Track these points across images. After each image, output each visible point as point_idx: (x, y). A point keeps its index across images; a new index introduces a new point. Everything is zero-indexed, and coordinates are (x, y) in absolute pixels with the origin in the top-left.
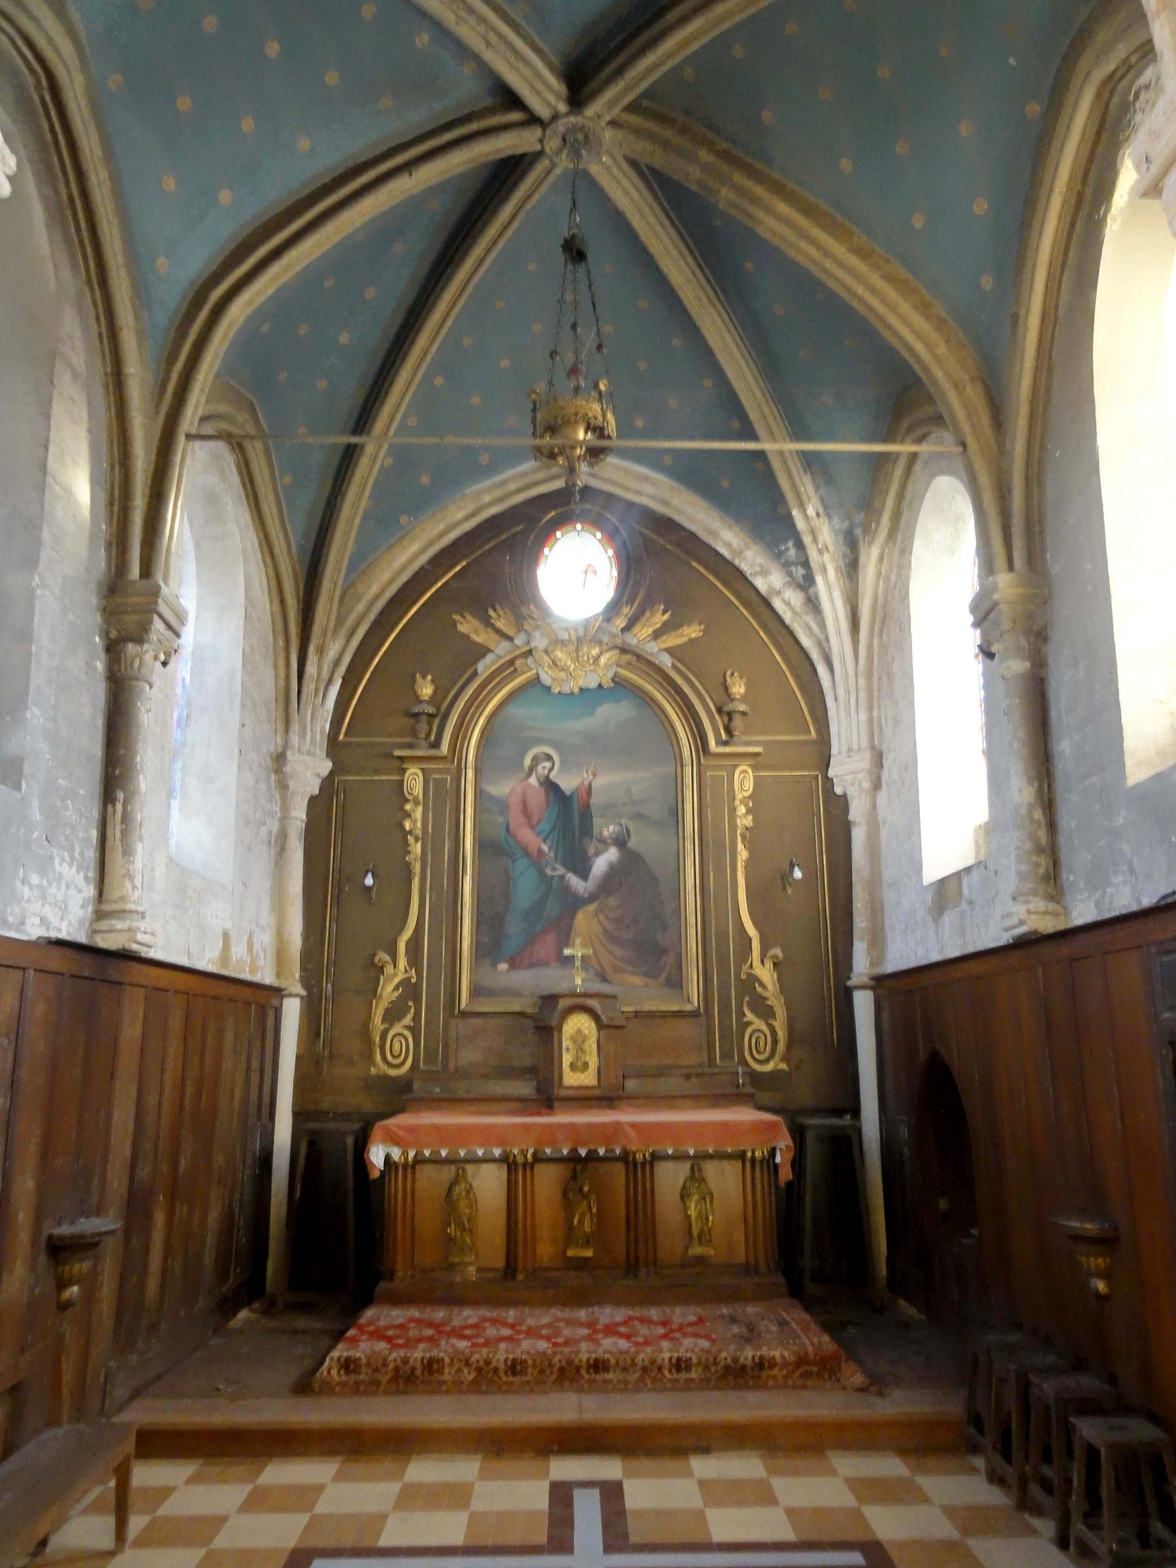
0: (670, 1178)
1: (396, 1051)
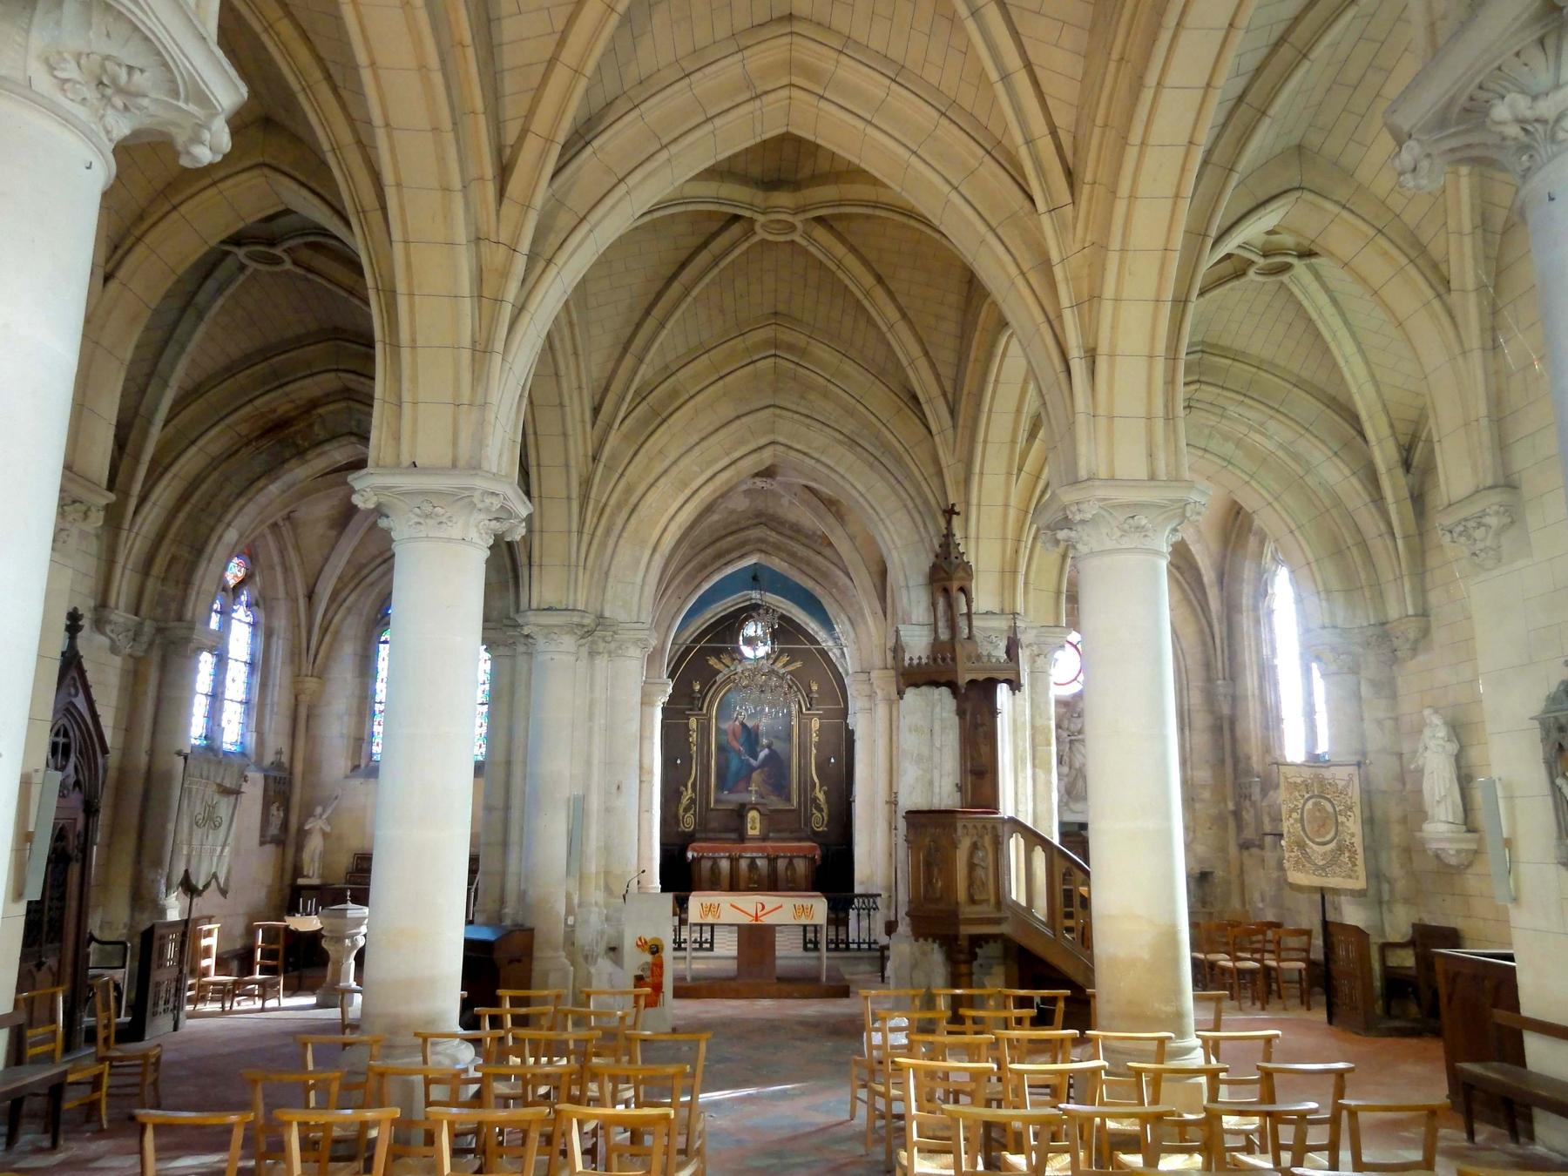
0: (782, 864)
1: (688, 822)
